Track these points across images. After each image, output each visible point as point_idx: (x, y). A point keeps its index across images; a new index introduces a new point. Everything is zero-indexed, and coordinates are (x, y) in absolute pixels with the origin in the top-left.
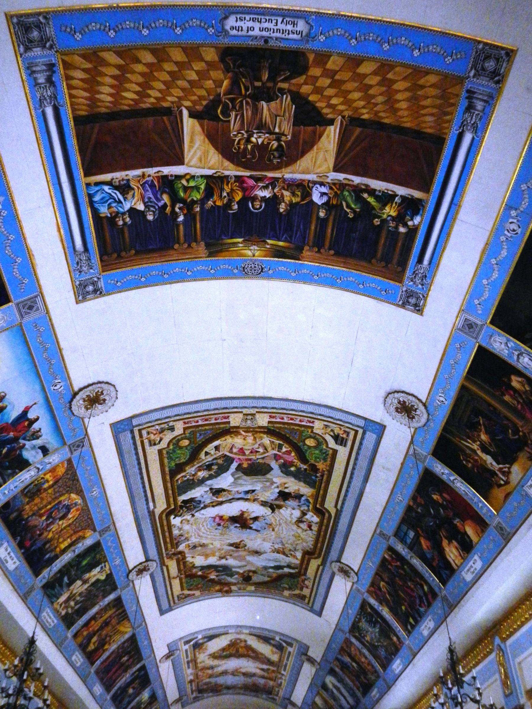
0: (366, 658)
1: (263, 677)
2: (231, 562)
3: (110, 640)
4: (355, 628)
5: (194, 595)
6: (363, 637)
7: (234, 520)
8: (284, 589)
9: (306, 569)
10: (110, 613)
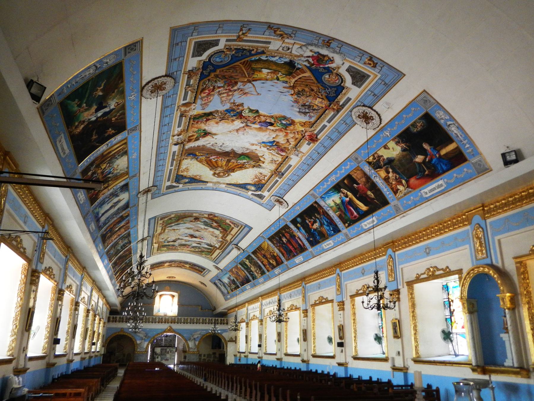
0: (115, 239)
1: (208, 116)
2: (203, 227)
3: (272, 253)
7: (196, 237)
10: (260, 256)
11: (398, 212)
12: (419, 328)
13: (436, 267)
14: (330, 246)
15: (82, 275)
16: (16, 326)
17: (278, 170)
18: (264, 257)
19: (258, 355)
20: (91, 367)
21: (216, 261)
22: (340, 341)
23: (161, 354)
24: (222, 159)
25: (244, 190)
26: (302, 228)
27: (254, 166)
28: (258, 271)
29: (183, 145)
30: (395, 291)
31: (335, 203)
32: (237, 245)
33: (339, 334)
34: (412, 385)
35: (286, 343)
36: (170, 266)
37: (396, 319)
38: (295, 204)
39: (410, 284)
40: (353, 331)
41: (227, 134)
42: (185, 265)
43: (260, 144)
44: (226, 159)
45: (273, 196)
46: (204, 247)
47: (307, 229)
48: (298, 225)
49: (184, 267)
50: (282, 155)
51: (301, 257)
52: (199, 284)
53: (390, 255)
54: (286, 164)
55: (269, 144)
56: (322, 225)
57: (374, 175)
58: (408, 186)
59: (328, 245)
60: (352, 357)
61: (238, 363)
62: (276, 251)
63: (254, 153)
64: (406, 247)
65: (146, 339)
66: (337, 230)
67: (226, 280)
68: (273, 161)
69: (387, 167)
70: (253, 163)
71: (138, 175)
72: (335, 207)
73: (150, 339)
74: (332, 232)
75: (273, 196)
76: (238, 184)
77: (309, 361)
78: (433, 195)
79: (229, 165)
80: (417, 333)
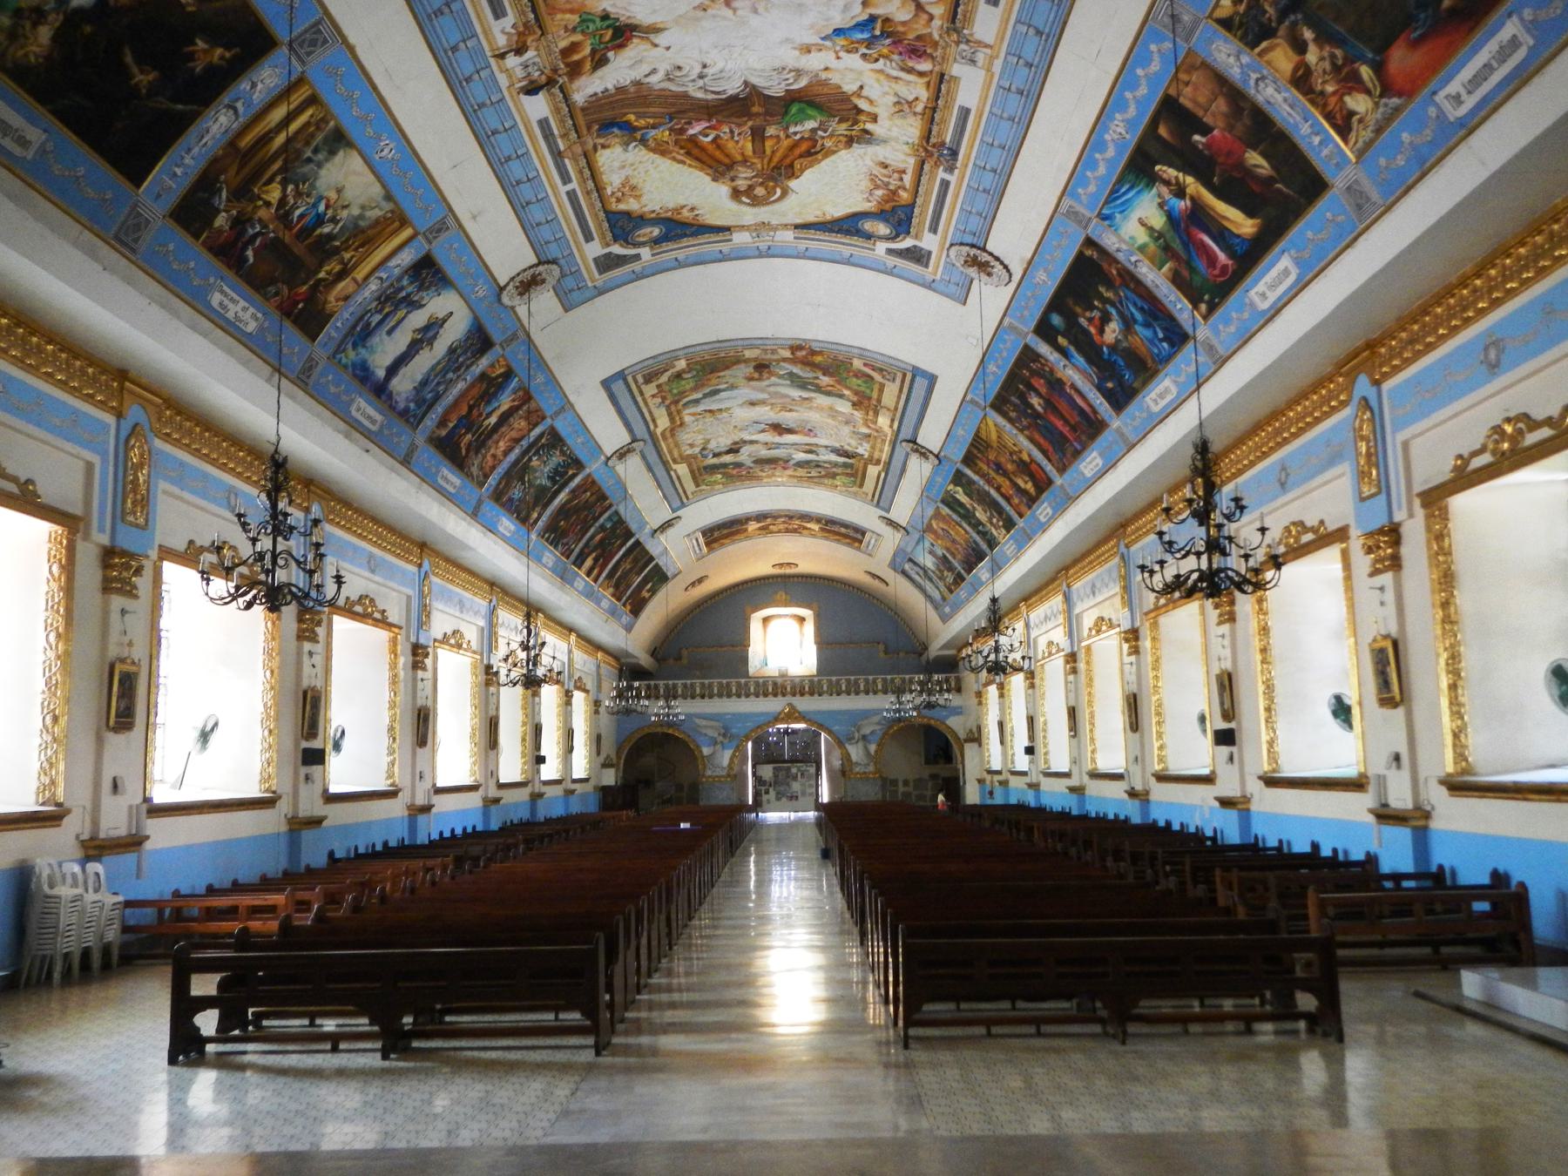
0: (506, 453)
2: (796, 393)
3: (1015, 452)
4: (555, 440)
5: (865, 365)
6: (537, 453)
7: (790, 431)
8: (689, 369)
9: (670, 415)
10: (985, 467)
11: (1366, 214)
12: (1469, 663)
13: (1525, 417)
14: (1169, 398)
15: (420, 566)
16: (55, 719)
17: (933, 140)
18: (997, 471)
19: (1027, 779)
20: (540, 824)
21: (882, 499)
22: (1223, 725)
23: (775, 783)
24: (732, 132)
25: (855, 240)
26: (1072, 349)
27: (850, 141)
28: (995, 520)
29: (561, 89)
30: (1381, 531)
31: (1151, 229)
32: (914, 442)
33: (1222, 704)
34: (1439, 876)
35: (1092, 739)
36: (765, 530)
37: (1386, 637)
38: (1029, 263)
39: (1435, 499)
40: (1261, 688)
41: (698, 19)
42: (809, 525)
43: (828, 43)
44: (746, 128)
45: (952, 245)
46: (830, 463)
47: (1090, 350)
48: (1061, 340)
49: (805, 532)
50: (921, 74)
51: (1094, 454)
52: (868, 580)
53: (1365, 399)
54: (948, 106)
55: (860, 36)
56: (1128, 324)
57: (1254, 76)
58: (1387, 89)
59: (1162, 396)
60: (1260, 778)
61: (989, 802)
62: (1026, 446)
63: (825, 83)
64: (1418, 355)
65: (726, 741)
66: (1178, 337)
67: (929, 562)
68: (902, 106)
69: (1294, 24)
70: (842, 128)
71: (451, 222)
72: (1152, 247)
73: (735, 743)
74: (1165, 345)
75: (952, 245)
76: (829, 222)
77: (1147, 793)
78: (1484, 100)
79: (768, 152)
80: (1460, 683)
